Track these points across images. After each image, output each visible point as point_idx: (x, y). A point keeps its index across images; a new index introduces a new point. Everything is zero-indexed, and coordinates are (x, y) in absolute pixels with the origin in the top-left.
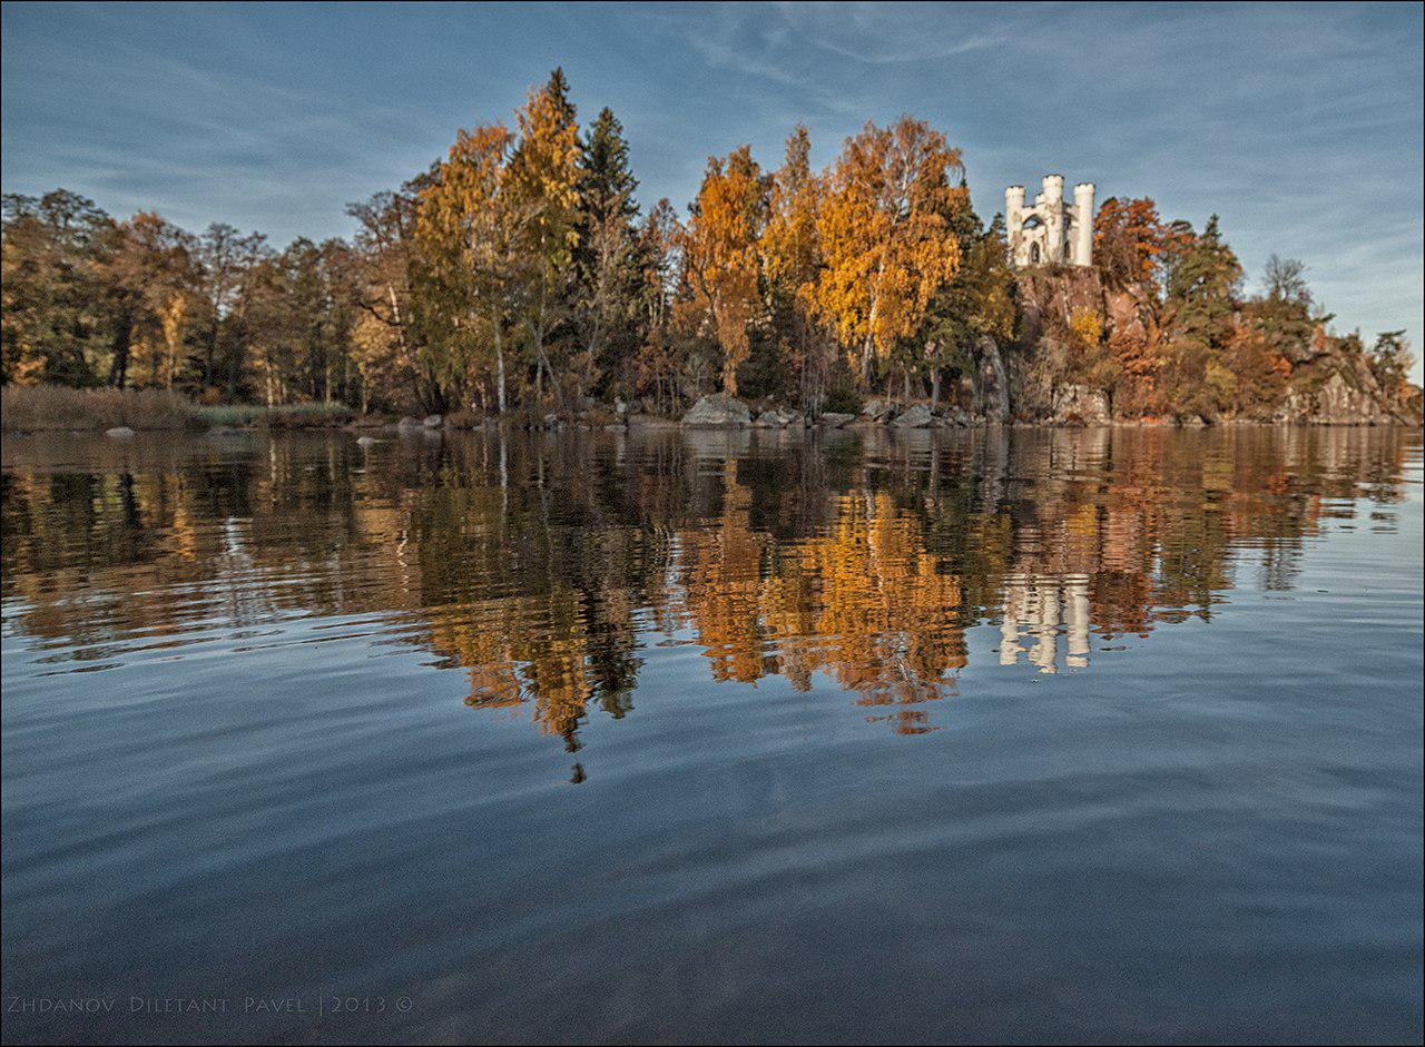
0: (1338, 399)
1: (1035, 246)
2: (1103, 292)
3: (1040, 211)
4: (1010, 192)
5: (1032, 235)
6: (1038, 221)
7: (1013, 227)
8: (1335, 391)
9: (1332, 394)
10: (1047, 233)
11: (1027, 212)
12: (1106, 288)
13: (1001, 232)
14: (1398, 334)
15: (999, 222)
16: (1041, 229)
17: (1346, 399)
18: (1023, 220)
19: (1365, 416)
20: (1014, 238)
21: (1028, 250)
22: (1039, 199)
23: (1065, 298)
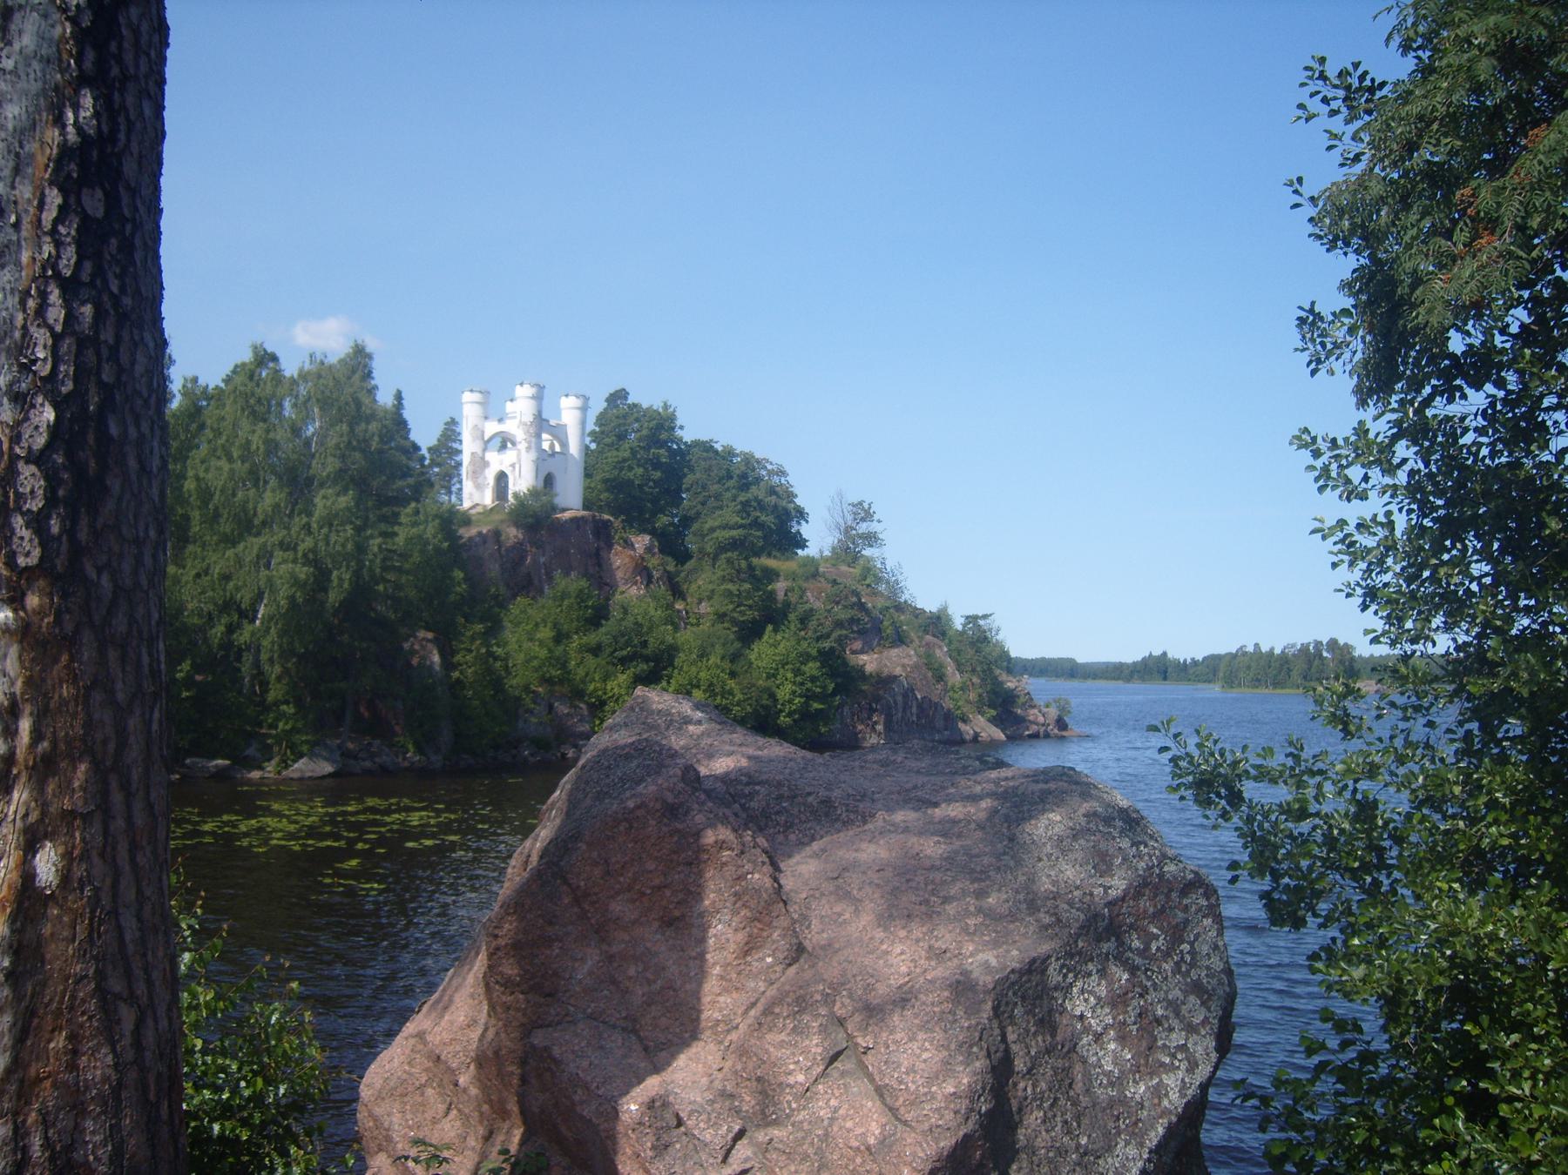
0: (904, 710)
1: (502, 478)
2: (598, 549)
3: (512, 427)
4: (467, 397)
5: (497, 461)
6: (505, 442)
7: (468, 447)
8: (900, 699)
9: (895, 702)
10: (519, 460)
11: (491, 428)
12: (602, 544)
13: (455, 445)
14: (985, 617)
15: (450, 434)
16: (510, 455)
17: (914, 710)
18: (486, 438)
19: (939, 732)
20: (472, 462)
21: (491, 481)
22: (509, 407)
23: (542, 560)
